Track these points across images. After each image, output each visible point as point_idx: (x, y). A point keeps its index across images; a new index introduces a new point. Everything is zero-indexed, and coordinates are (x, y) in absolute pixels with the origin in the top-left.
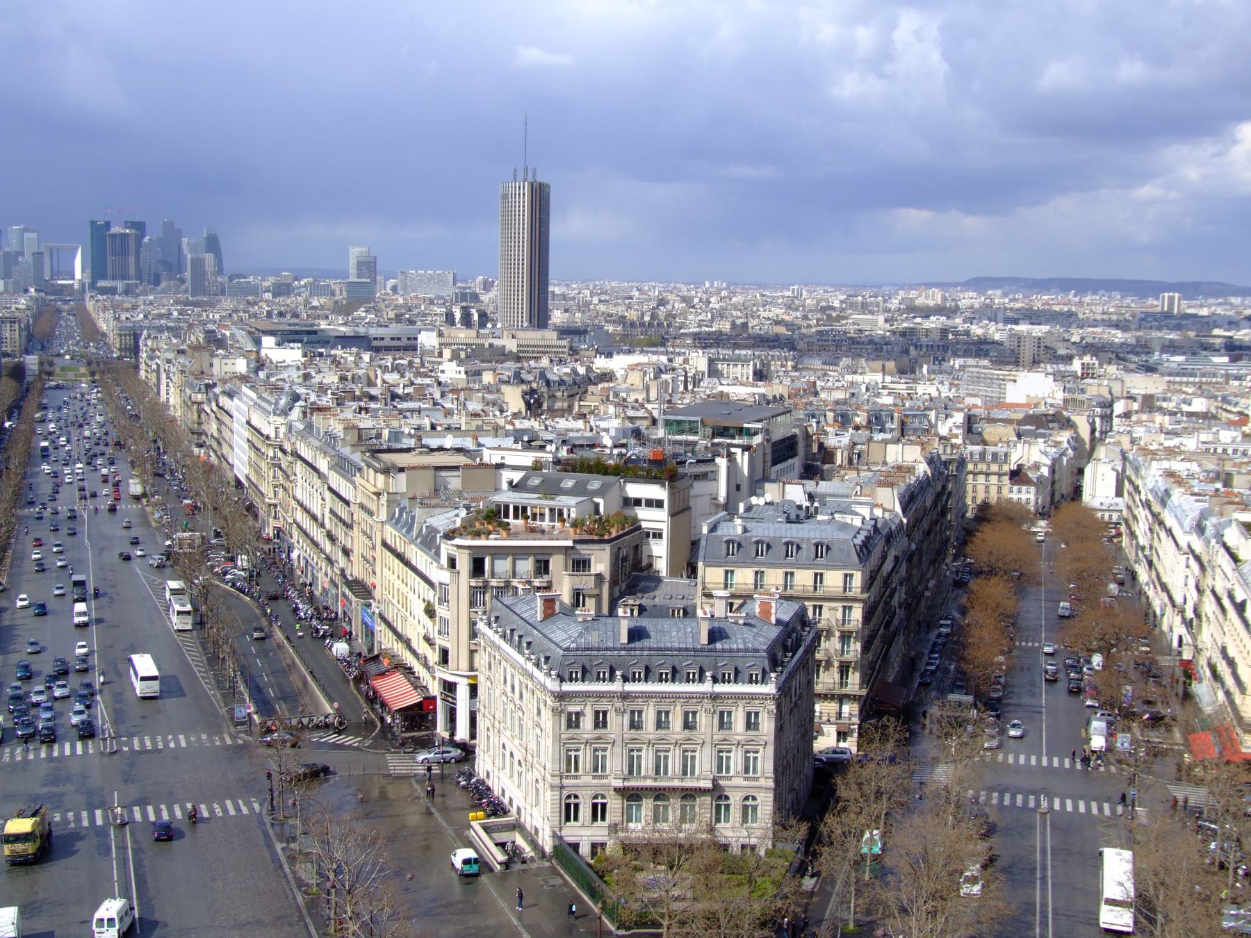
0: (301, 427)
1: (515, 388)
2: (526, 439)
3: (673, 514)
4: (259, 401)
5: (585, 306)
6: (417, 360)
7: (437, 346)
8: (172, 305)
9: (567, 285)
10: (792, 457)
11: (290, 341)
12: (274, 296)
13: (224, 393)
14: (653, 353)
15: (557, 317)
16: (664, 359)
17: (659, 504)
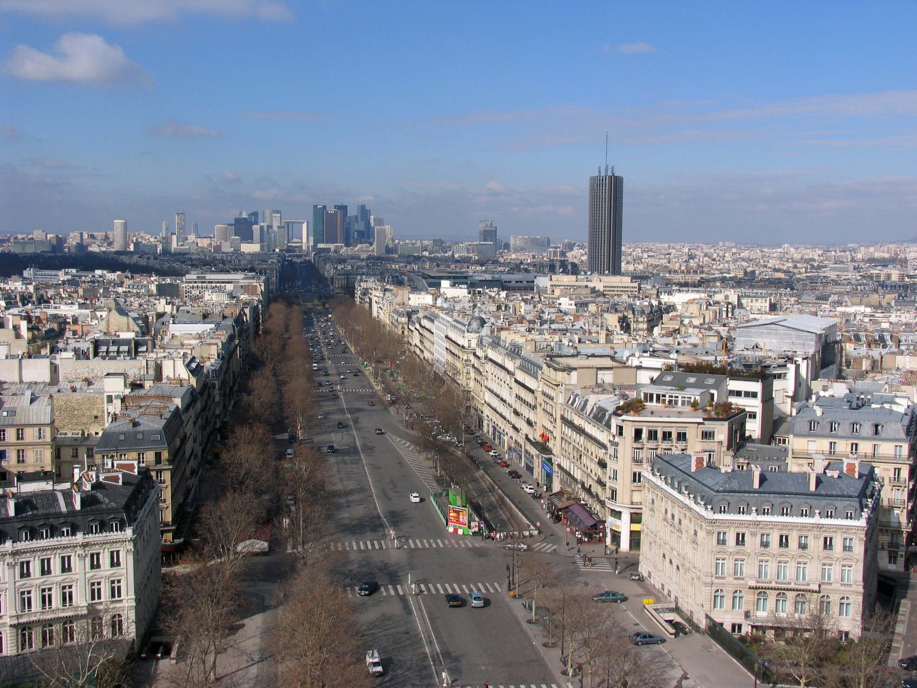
4: (454, 323)
13: (425, 317)
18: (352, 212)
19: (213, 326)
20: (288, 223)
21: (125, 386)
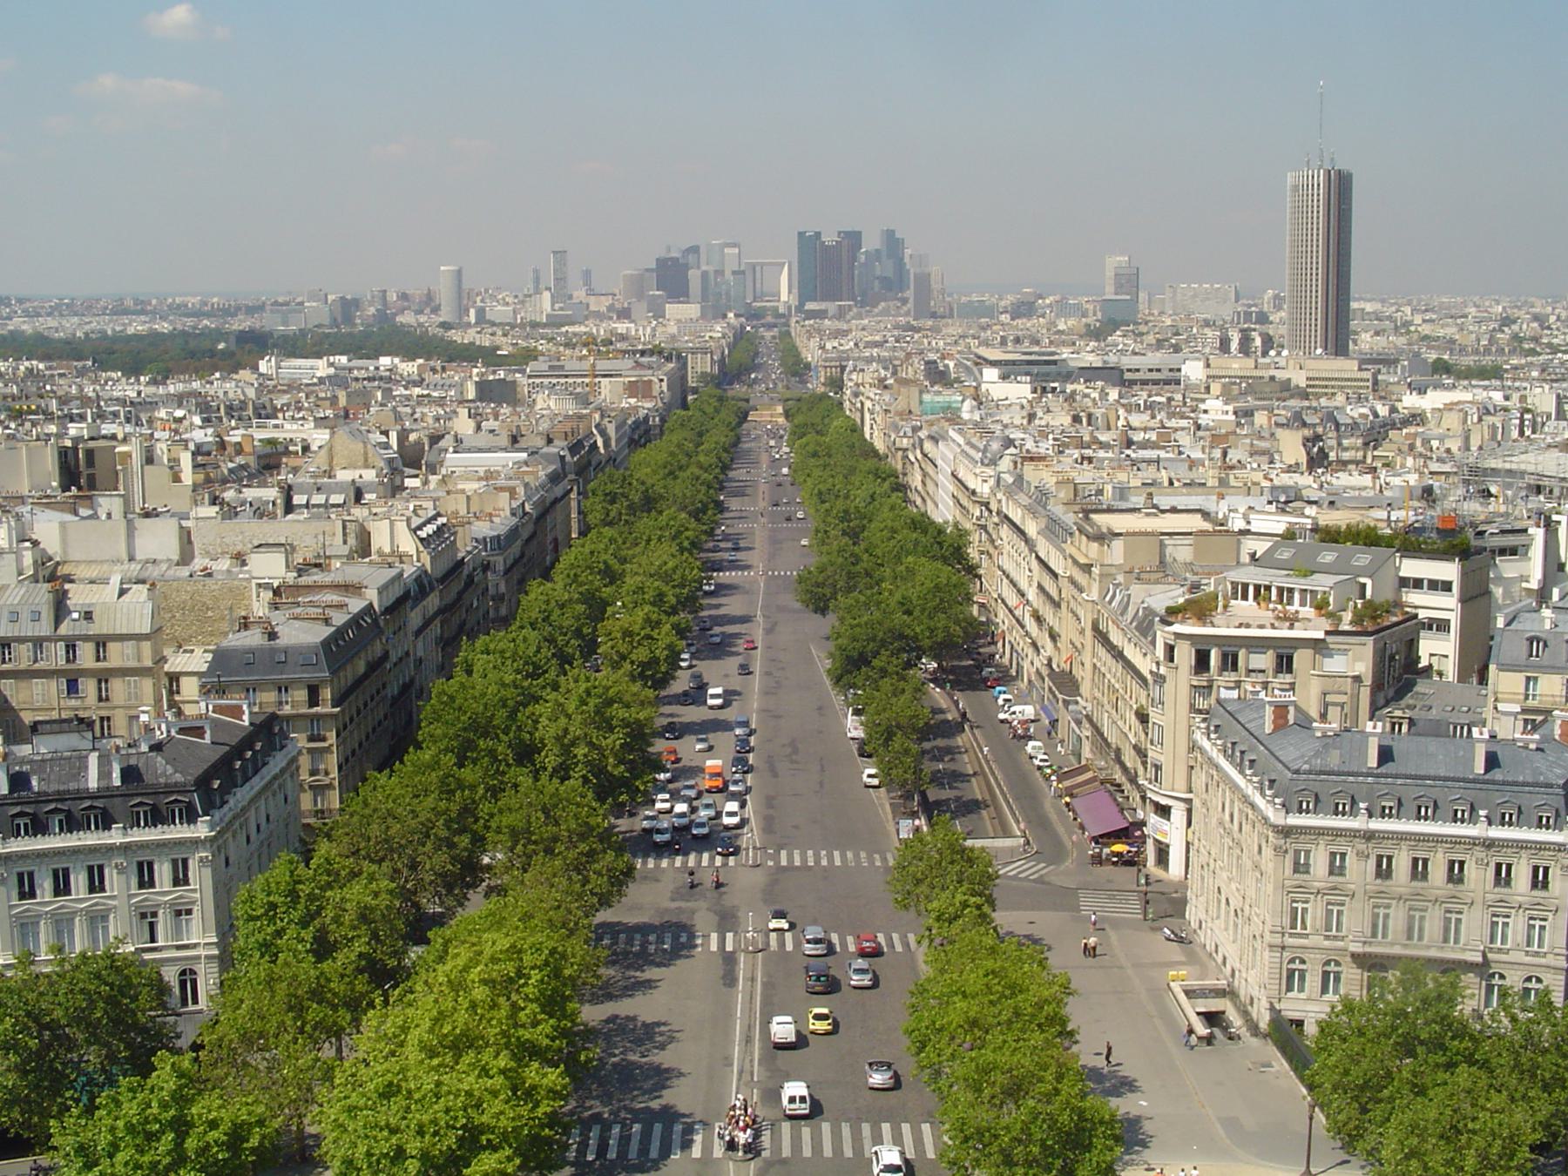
0: (1011, 480)
1: (1294, 432)
2: (1283, 499)
3: (1464, 600)
5: (1403, 327)
6: (1179, 397)
7: (1204, 379)
8: (889, 331)
9: (1383, 301)
12: (1013, 319)
13: (931, 438)
14: (1486, 388)
15: (1366, 341)
18: (871, 242)
19: (524, 455)
20: (754, 267)
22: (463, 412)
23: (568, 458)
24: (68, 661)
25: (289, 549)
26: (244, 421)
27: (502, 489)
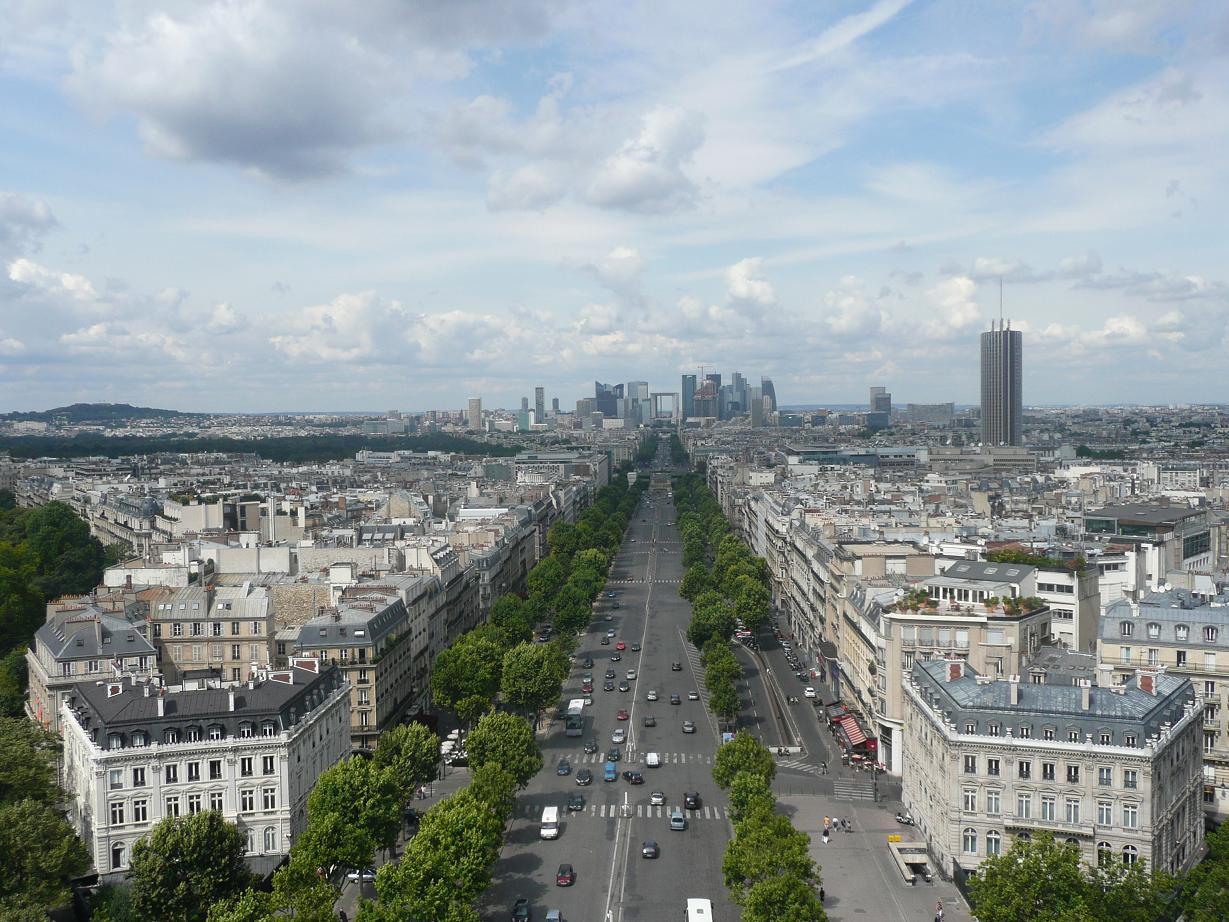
4: (773, 505)
10: (1205, 551)
11: (809, 459)
13: (754, 498)
16: (1119, 470)
17: (1069, 589)
18: (726, 381)
21: (352, 576)
22: (474, 484)
23: (533, 511)
24: (215, 634)
25: (353, 566)
26: (342, 488)
27: (491, 531)
